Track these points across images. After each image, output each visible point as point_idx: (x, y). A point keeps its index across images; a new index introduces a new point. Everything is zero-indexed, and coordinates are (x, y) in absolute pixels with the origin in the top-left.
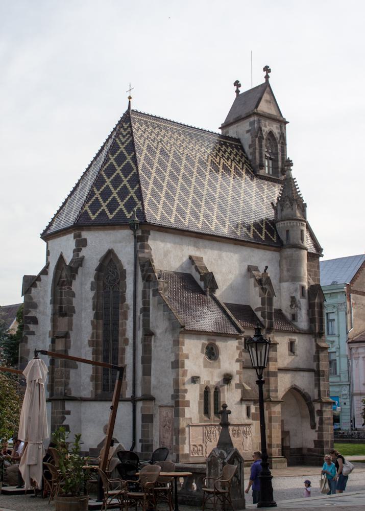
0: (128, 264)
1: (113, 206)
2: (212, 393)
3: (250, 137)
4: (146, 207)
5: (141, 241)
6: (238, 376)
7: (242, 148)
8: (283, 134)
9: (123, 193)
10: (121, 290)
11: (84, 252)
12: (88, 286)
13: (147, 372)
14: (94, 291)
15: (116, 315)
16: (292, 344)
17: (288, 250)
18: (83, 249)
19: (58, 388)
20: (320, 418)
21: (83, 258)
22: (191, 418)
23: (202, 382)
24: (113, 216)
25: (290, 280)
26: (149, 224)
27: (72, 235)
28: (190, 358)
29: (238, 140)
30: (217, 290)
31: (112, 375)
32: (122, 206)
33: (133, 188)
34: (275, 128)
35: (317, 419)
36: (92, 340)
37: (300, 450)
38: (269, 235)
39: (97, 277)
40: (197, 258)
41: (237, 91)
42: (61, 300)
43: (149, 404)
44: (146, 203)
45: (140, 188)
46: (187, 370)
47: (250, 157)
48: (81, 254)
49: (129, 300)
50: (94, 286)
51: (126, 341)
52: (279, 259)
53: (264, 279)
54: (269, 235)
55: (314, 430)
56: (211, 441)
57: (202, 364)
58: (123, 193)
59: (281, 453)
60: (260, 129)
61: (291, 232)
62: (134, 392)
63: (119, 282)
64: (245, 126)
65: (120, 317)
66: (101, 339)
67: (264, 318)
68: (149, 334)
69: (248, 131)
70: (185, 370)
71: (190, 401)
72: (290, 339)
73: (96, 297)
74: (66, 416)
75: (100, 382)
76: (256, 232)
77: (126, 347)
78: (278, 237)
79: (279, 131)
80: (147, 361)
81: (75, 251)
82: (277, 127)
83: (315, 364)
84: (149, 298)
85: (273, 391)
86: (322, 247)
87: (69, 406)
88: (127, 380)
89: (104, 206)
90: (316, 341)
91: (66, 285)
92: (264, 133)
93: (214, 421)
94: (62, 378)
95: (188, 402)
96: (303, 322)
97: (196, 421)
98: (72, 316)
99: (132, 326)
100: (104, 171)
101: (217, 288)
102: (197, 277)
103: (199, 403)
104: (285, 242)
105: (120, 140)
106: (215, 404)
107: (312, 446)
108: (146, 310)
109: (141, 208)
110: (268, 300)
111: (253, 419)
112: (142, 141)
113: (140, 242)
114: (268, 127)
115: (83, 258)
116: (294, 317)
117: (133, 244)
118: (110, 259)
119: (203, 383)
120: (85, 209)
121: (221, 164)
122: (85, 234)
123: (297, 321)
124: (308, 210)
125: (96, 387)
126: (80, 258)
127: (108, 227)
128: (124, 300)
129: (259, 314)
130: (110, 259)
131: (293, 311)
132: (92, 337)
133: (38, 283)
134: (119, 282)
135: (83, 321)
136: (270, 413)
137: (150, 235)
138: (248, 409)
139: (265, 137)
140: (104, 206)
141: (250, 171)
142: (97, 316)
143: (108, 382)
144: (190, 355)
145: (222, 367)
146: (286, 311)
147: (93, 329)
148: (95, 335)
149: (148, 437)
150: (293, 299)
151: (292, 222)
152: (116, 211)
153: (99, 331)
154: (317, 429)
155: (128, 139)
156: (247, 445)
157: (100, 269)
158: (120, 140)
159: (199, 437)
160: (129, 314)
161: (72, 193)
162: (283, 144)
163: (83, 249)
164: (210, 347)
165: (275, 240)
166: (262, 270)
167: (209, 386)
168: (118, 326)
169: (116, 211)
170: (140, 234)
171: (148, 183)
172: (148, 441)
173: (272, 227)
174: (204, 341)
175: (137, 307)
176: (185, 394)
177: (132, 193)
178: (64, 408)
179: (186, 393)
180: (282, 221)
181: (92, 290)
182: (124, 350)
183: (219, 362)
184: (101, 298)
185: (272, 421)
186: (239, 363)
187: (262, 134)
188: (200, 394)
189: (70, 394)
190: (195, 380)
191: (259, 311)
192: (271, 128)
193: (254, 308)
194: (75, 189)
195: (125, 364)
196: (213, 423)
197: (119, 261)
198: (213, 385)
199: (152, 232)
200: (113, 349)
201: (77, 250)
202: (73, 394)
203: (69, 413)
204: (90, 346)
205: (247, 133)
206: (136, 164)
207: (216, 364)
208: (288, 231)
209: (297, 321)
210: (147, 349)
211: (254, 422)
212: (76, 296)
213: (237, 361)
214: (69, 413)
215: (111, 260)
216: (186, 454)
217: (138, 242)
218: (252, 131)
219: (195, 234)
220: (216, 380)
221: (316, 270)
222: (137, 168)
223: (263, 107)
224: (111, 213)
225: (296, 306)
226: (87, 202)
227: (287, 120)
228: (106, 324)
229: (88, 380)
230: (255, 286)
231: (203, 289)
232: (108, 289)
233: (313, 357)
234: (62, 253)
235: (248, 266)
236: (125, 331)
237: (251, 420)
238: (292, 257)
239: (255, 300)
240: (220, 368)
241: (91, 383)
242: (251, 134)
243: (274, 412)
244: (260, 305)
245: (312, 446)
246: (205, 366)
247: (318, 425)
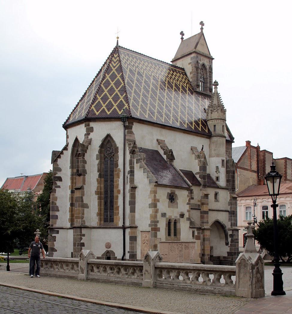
0: (120, 143)
1: (110, 106)
2: (172, 224)
3: (191, 67)
4: (131, 107)
5: (128, 128)
7: (186, 74)
8: (211, 66)
9: (116, 98)
10: (115, 160)
11: (92, 136)
12: (95, 157)
13: (133, 210)
14: (98, 161)
15: (112, 175)
16: (216, 194)
17: (215, 137)
18: (91, 133)
19: (77, 220)
20: (231, 239)
21: (91, 139)
22: (161, 238)
23: (167, 217)
24: (110, 112)
25: (216, 156)
26: (134, 118)
27: (84, 125)
29: (183, 69)
30: (174, 161)
31: (110, 212)
32: (115, 106)
33: (122, 95)
34: (206, 62)
35: (230, 239)
36: (97, 191)
37: (219, 257)
38: (204, 128)
39: (100, 152)
40: (161, 140)
41: (182, 38)
42: (78, 165)
43: (134, 230)
44: (131, 105)
45: (126, 95)
46: (158, 209)
47: (191, 80)
48: (90, 137)
49: (121, 166)
50: (98, 157)
51: (119, 192)
52: (209, 143)
53: (201, 155)
54: (204, 128)
55: (228, 246)
56: (172, 252)
57: (167, 206)
58: (116, 98)
59: (209, 259)
60: (197, 62)
61: (216, 126)
62: (124, 223)
63: (114, 154)
64: (188, 59)
65: (115, 177)
66: (103, 190)
67: (201, 179)
68: (134, 188)
69: (190, 64)
72: (215, 192)
73: (100, 164)
74: (82, 237)
75: (102, 217)
76: (196, 126)
77: (119, 195)
78: (209, 129)
79: (208, 64)
80: (133, 203)
81: (85, 135)
82: (207, 61)
83: (229, 207)
84: (134, 165)
85: (205, 223)
86: (234, 137)
87: (84, 231)
88: (119, 215)
89: (104, 106)
90: (230, 193)
91: (81, 156)
92: (199, 65)
94: (80, 214)
95: (159, 228)
96: (222, 182)
98: (85, 175)
99: (122, 182)
100: (104, 84)
101: (174, 159)
102: (162, 152)
104: (213, 133)
105: (112, 65)
106: (174, 230)
107: (226, 255)
108: (132, 172)
109: (128, 108)
110: (203, 167)
111: (196, 239)
112: (126, 66)
113: (128, 129)
114: (202, 61)
115: (91, 139)
116: (217, 178)
117: (123, 130)
118: (108, 141)
119: (168, 217)
120: (92, 108)
121: (174, 83)
122: (92, 124)
123: (219, 181)
124: (227, 113)
125: (100, 220)
126: (89, 139)
127: (107, 120)
128: (117, 165)
129: (197, 176)
130: (108, 141)
131: (217, 175)
132: (98, 189)
133: (61, 155)
134: (114, 154)
135: (92, 179)
136: (204, 236)
137: (133, 125)
138: (193, 232)
139: (200, 67)
140: (104, 106)
141: (191, 88)
142: (100, 176)
143: (107, 216)
144: (160, 199)
146: (213, 175)
147: (98, 184)
148: (99, 188)
149: (134, 250)
150: (217, 167)
151: (217, 120)
152: (112, 110)
153: (101, 185)
154: (229, 245)
155: (118, 64)
157: (102, 146)
158: (112, 65)
159: (165, 250)
160: (120, 174)
161: (82, 99)
162: (210, 73)
163: (91, 133)
164: (172, 195)
165: (207, 131)
166: (200, 150)
167: (171, 219)
168: (114, 183)
169: (112, 110)
170: (127, 124)
171: (131, 93)
172: (134, 252)
173: (205, 123)
174: (169, 190)
175: (125, 170)
177: (122, 98)
178: (81, 232)
179: (158, 223)
180: (212, 119)
181: (97, 159)
182: (117, 197)
184: (103, 165)
185: (205, 240)
186: (188, 205)
187: (198, 65)
189: (85, 224)
190: (164, 215)
191: (198, 174)
192: (204, 62)
193: (194, 173)
194: (84, 96)
195: (118, 205)
196: (173, 241)
197: (114, 141)
199: (134, 123)
200: (110, 196)
201: (87, 134)
202: (87, 224)
203: (84, 235)
204: (96, 194)
205: (189, 65)
206: (123, 81)
208: (215, 126)
209: (219, 181)
210: (133, 196)
211: (196, 241)
212: (87, 163)
213: (188, 204)
214: (84, 235)
215: (109, 141)
217: (126, 129)
218: (192, 63)
219: (160, 126)
220: (176, 215)
221: (230, 151)
222: (124, 82)
223: (200, 49)
224: (109, 111)
225: (219, 172)
226: (92, 103)
227: (213, 57)
228: (106, 181)
229: (96, 215)
230: (195, 159)
231: (166, 160)
232: (106, 159)
233: (228, 203)
234: (77, 136)
235: (191, 147)
236: (118, 185)
238: (217, 142)
239: (195, 169)
241: (97, 217)
242: (192, 65)
243: (207, 235)
244: (198, 171)
245: (226, 255)
246: (169, 207)
247: (230, 243)
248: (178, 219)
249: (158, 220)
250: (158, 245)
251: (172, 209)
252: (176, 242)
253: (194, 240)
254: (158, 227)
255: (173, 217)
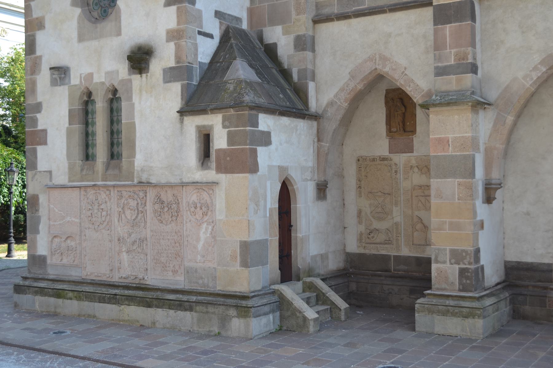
6: (172, 45)
22: (50, 172)
23: (75, 80)
28: (47, 24)
70: (37, 57)
71: (48, 131)
93: (104, 179)
95: (45, 131)
97: (61, 178)
103: (69, 133)
111: (220, 169)
145: (124, 30)
156: (200, 246)
159: (68, 219)
176: (38, 116)
179: (39, 112)
183: (118, 19)
188: (70, 111)
198: (103, 83)
207: (108, 25)
211: (223, 178)
216: (40, 256)
220: (109, 69)
237: (214, 172)
240: (119, 34)
243: (443, 142)
246: (81, 38)
248: (122, 81)
249: (39, 100)
250: (42, 199)
251: (94, 44)
252: (114, 186)
253: (211, 175)
254: (40, 127)
255: (98, 78)
